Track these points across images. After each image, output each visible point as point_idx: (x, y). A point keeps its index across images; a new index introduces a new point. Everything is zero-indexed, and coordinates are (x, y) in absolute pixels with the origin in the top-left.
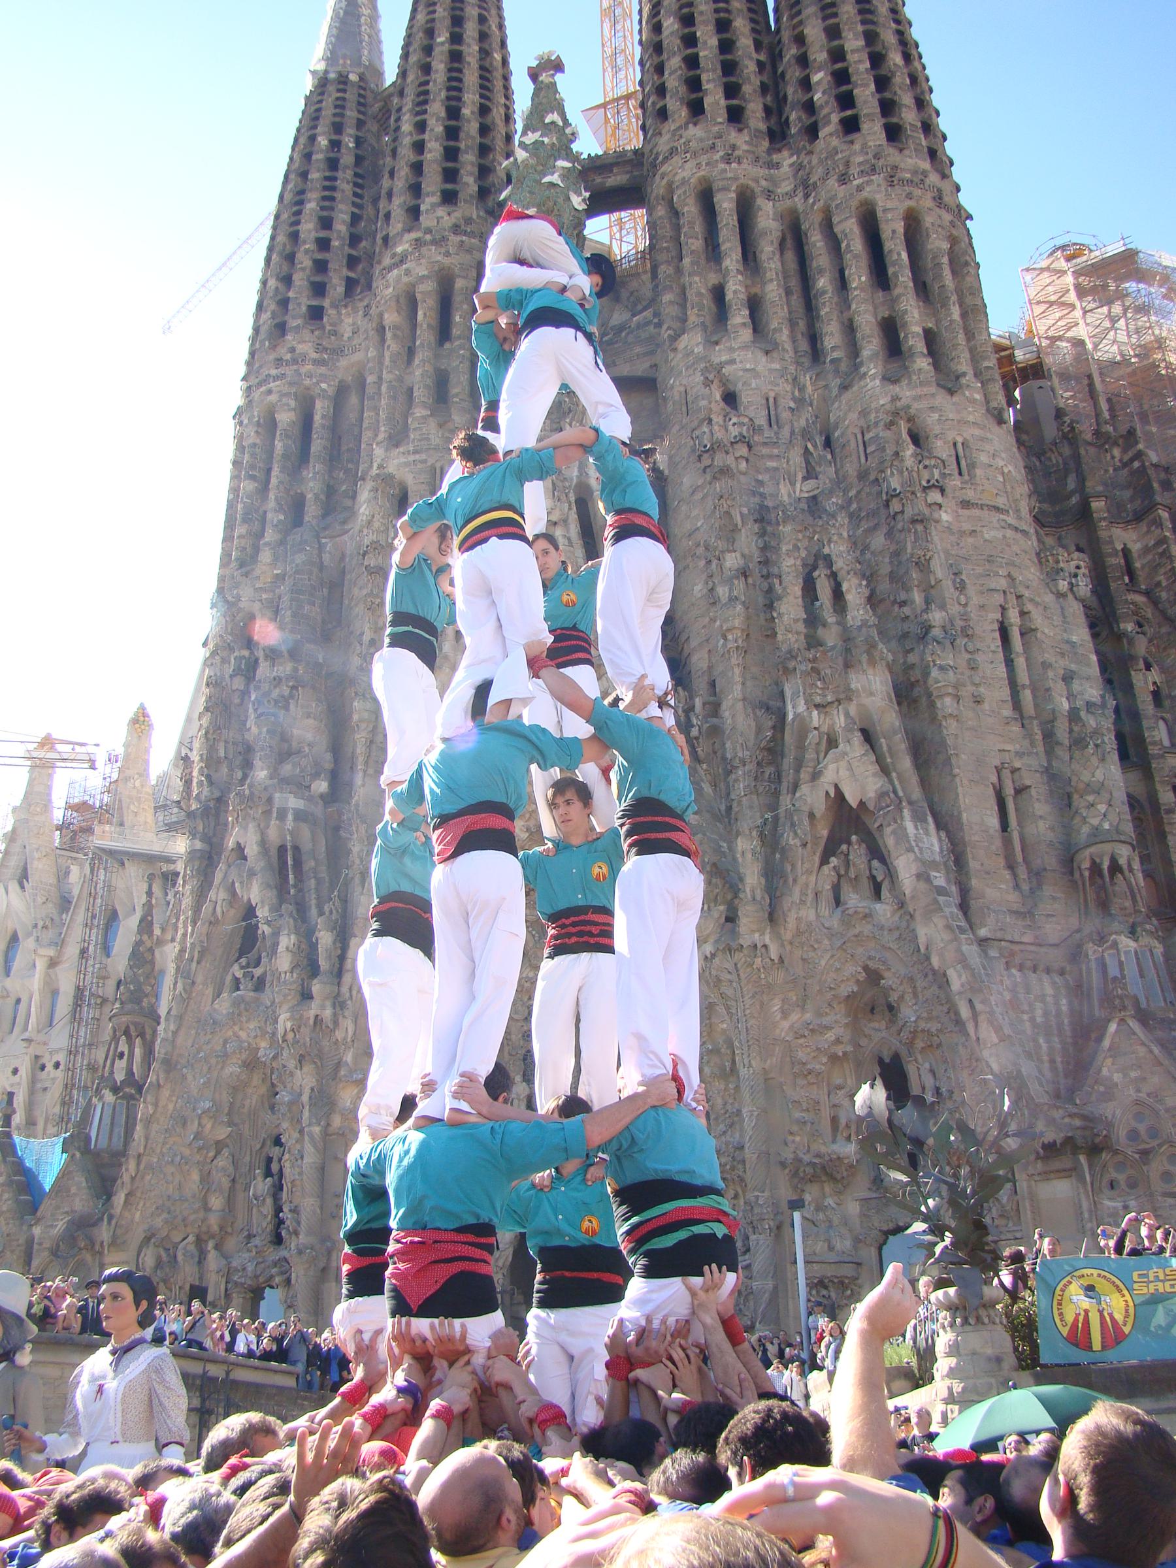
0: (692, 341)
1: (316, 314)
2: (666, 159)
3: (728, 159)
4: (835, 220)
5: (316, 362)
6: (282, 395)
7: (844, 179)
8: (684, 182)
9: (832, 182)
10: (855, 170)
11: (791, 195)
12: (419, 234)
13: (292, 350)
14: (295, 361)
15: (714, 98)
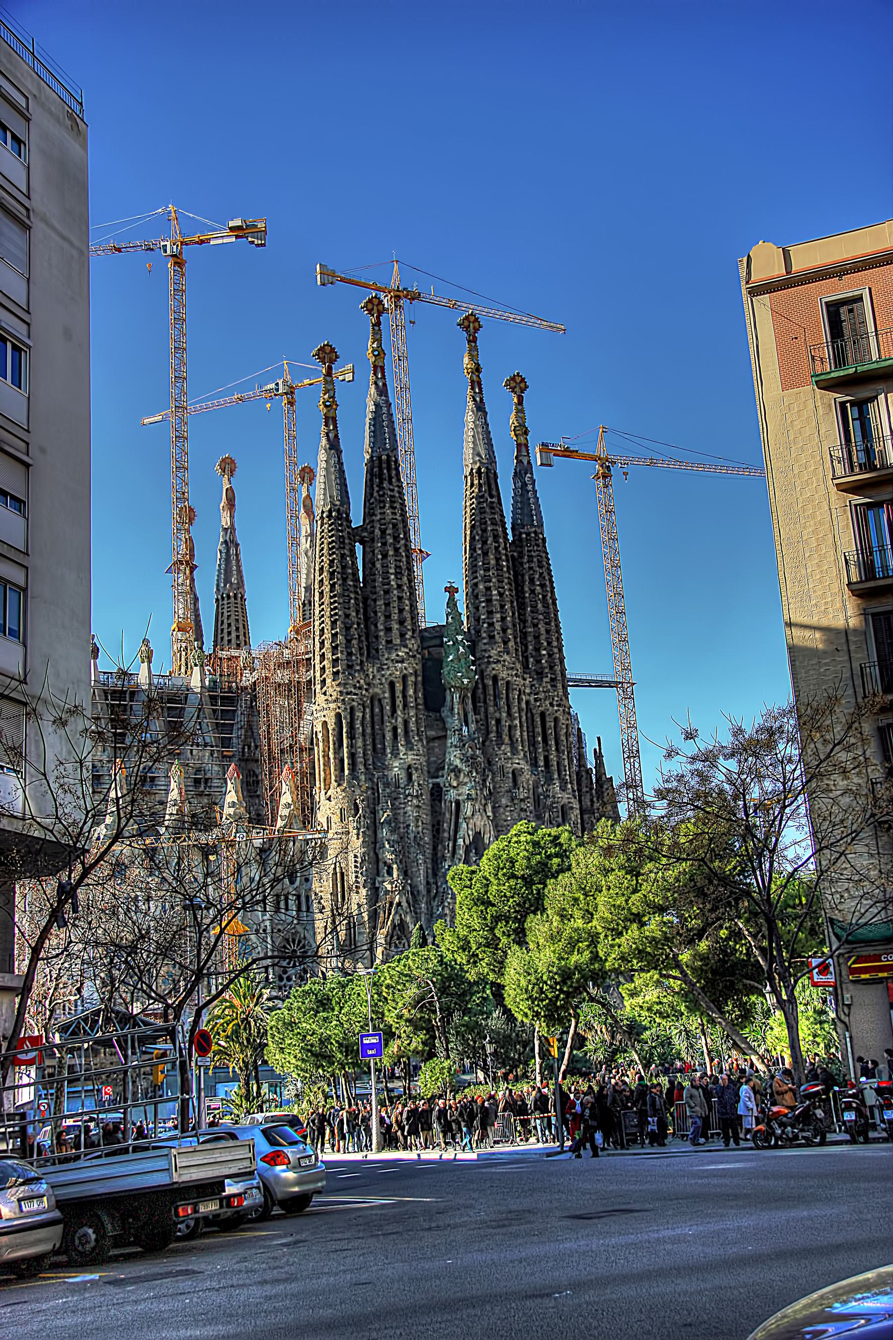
0: (506, 748)
1: (362, 662)
2: (495, 663)
3: (516, 675)
4: (548, 719)
5: (366, 690)
6: (359, 704)
7: (551, 705)
8: (503, 679)
9: (547, 702)
10: (555, 703)
11: (529, 694)
12: (407, 650)
13: (358, 682)
14: (360, 688)
15: (511, 644)
